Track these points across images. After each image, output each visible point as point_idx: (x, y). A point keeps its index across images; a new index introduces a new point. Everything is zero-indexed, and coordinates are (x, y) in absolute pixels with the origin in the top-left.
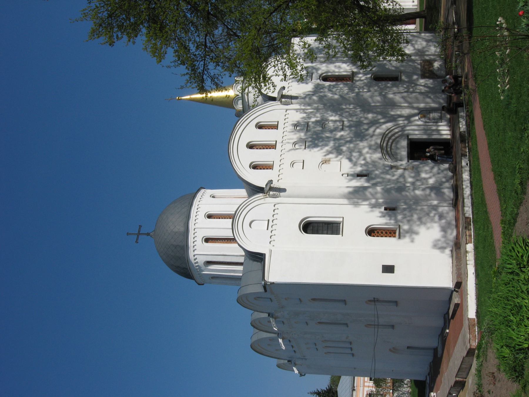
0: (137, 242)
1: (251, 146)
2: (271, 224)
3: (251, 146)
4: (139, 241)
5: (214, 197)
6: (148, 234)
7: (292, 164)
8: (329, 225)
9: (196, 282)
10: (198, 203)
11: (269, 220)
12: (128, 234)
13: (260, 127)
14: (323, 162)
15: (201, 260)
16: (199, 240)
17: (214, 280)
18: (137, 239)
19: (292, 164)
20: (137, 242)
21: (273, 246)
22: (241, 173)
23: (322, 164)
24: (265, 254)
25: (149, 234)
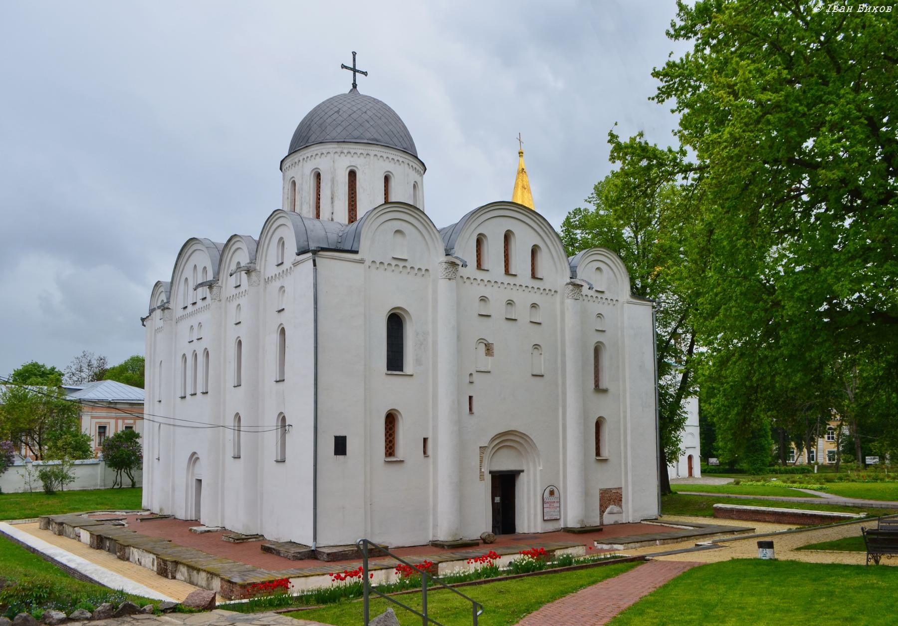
1: (508, 236)
3: (508, 236)
5: (414, 186)
6: (355, 86)
10: (406, 161)
12: (354, 54)
13: (534, 251)
17: (289, 186)
19: (483, 299)
25: (356, 88)
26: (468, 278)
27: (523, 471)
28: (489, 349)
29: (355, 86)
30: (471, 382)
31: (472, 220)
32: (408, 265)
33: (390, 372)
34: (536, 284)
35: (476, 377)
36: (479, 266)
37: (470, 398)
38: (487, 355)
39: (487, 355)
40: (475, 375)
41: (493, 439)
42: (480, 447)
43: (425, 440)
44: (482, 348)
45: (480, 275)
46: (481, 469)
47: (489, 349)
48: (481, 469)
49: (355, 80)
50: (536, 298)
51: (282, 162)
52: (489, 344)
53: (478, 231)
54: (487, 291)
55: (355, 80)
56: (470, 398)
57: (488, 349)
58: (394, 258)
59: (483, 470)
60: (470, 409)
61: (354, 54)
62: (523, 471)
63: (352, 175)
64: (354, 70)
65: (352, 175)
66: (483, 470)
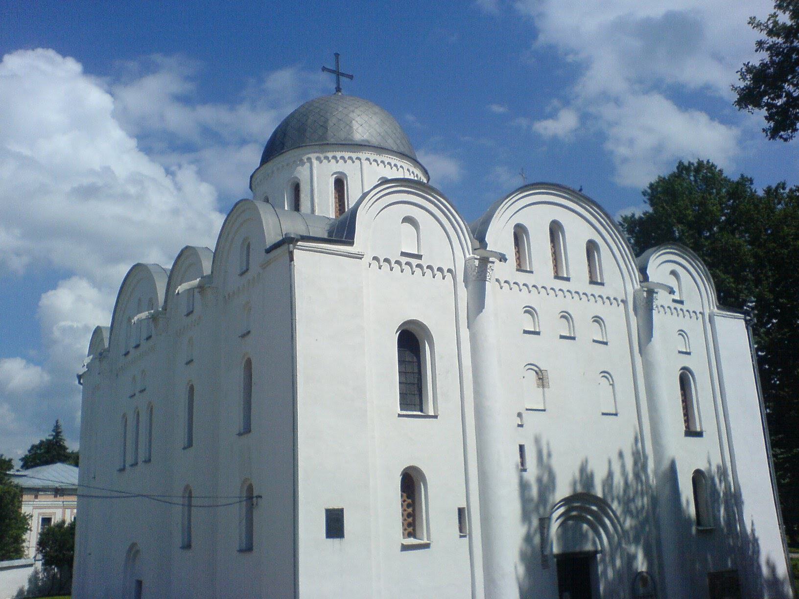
2: (414, 262)
3: (555, 229)
7: (530, 311)
8: (416, 386)
9: (257, 169)
11: (419, 257)
13: (592, 248)
14: (540, 373)
15: (302, 173)
16: (340, 167)
19: (530, 311)
21: (370, 264)
22: (503, 210)
23: (536, 372)
24: (351, 243)
26: (506, 282)
28: (542, 378)
30: (521, 426)
31: (503, 210)
32: (424, 262)
34: (596, 290)
36: (520, 268)
40: (525, 414)
45: (522, 278)
50: (599, 309)
51: (252, 177)
52: (541, 371)
53: (517, 220)
54: (533, 299)
58: (403, 254)
63: (340, 184)
65: (340, 184)
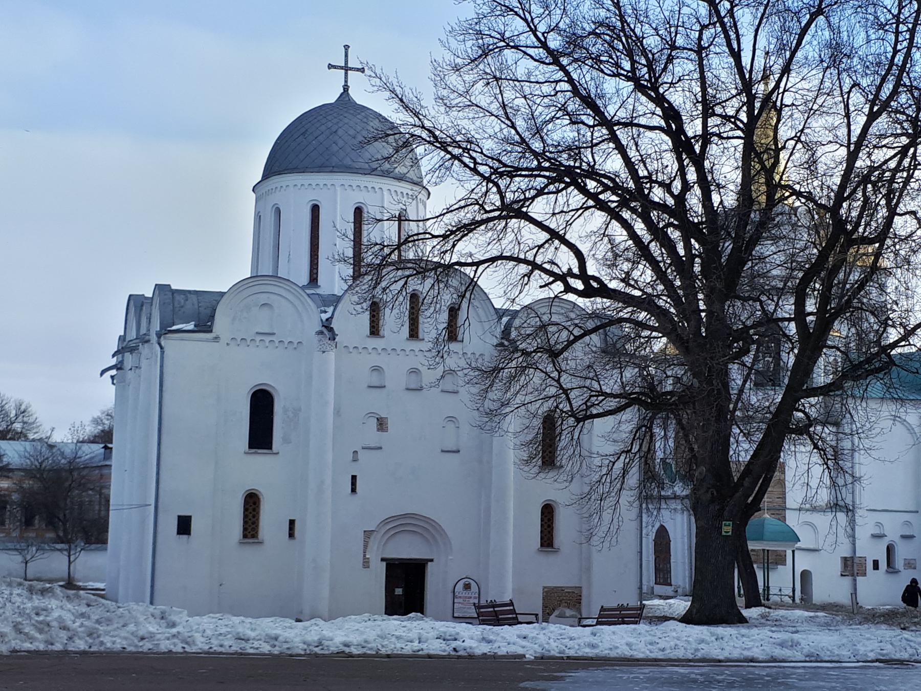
0: (331, 66)
4: (333, 70)
6: (346, 88)
12: (347, 47)
18: (335, 67)
20: (331, 66)
27: (432, 560)
28: (382, 424)
29: (346, 88)
33: (253, 451)
35: (362, 455)
37: (354, 478)
38: (378, 430)
39: (378, 430)
41: (386, 522)
42: (365, 531)
43: (292, 523)
44: (374, 423)
46: (365, 556)
47: (382, 424)
48: (365, 556)
49: (346, 81)
52: (381, 418)
55: (346, 81)
56: (354, 478)
57: (381, 424)
59: (367, 556)
60: (354, 490)
61: (347, 47)
62: (432, 560)
64: (346, 69)
66: (367, 556)
